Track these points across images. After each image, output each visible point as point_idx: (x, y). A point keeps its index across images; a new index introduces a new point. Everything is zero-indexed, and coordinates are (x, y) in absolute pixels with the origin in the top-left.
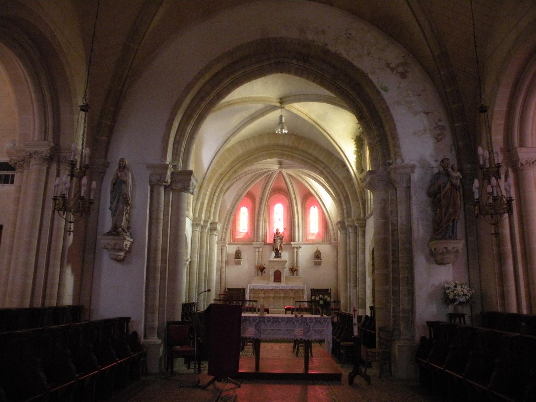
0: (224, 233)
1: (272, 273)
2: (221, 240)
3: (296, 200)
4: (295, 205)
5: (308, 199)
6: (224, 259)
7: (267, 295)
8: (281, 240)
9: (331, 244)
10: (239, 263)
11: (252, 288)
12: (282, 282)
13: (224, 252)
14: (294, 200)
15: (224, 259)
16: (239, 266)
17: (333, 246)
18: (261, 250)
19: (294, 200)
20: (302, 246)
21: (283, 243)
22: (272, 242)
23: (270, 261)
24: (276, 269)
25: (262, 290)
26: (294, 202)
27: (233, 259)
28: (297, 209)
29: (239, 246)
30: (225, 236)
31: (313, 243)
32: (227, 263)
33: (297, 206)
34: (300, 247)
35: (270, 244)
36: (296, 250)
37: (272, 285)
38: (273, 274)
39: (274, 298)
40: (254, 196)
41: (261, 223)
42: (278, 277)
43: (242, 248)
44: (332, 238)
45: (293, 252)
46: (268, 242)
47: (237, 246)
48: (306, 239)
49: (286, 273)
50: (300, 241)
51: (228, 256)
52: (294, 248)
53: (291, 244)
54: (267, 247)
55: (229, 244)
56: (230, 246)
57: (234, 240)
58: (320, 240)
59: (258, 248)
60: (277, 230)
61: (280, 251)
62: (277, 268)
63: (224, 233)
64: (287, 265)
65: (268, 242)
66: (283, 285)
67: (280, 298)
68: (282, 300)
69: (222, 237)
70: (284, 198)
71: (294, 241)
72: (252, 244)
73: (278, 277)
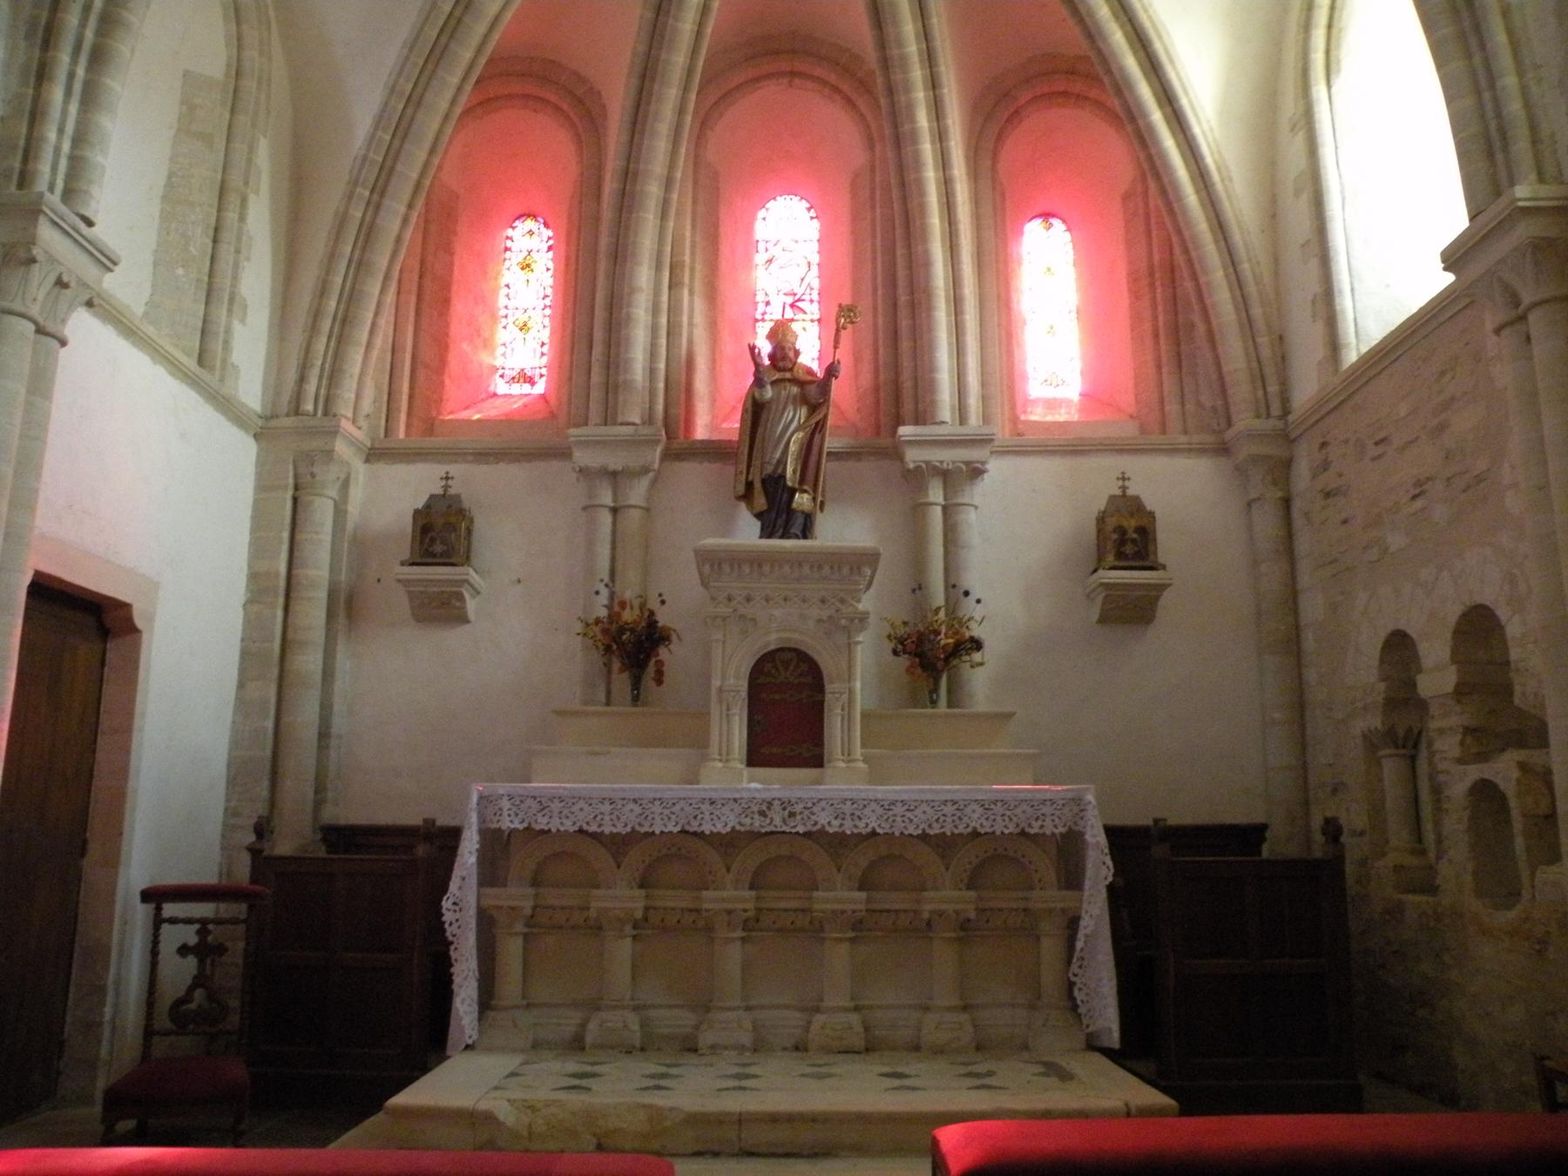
0: (320, 345)
1: (731, 675)
2: (296, 410)
3: (934, 84)
4: (923, 119)
5: (1015, 117)
6: (318, 570)
7: (673, 900)
8: (813, 408)
9: (1223, 450)
10: (442, 609)
11: (507, 823)
12: (837, 762)
13: (322, 511)
14: (917, 74)
15: (318, 570)
16: (452, 638)
17: (1240, 471)
18: (637, 493)
19: (917, 74)
20: (997, 468)
21: (832, 443)
22: (732, 427)
23: (713, 563)
24: (772, 640)
25: (618, 845)
26: (920, 95)
27: (394, 572)
28: (944, 163)
29: (455, 469)
30: (334, 375)
31: (1066, 445)
32: (347, 607)
33: (941, 136)
34: (975, 472)
35: (714, 451)
36: (936, 494)
37: (728, 783)
38: (739, 683)
39: (751, 925)
40: (594, 93)
41: (643, 276)
42: (788, 712)
43: (476, 483)
44: (1241, 392)
45: (919, 510)
46: (701, 432)
47: (439, 470)
48: (1015, 420)
49: (861, 675)
50: (974, 418)
51: (358, 547)
52: (916, 478)
53: (894, 452)
54: (694, 477)
55: (374, 455)
56: (385, 470)
57: (430, 428)
58: (1129, 430)
59: (613, 476)
60: (780, 334)
61: (802, 500)
62: (783, 623)
63: (320, 345)
64: (877, 603)
65: (701, 432)
66: (860, 781)
67: (814, 929)
68: (839, 956)
69: (302, 380)
70: (834, 126)
71: (919, 420)
72: (564, 454)
73: (788, 712)
